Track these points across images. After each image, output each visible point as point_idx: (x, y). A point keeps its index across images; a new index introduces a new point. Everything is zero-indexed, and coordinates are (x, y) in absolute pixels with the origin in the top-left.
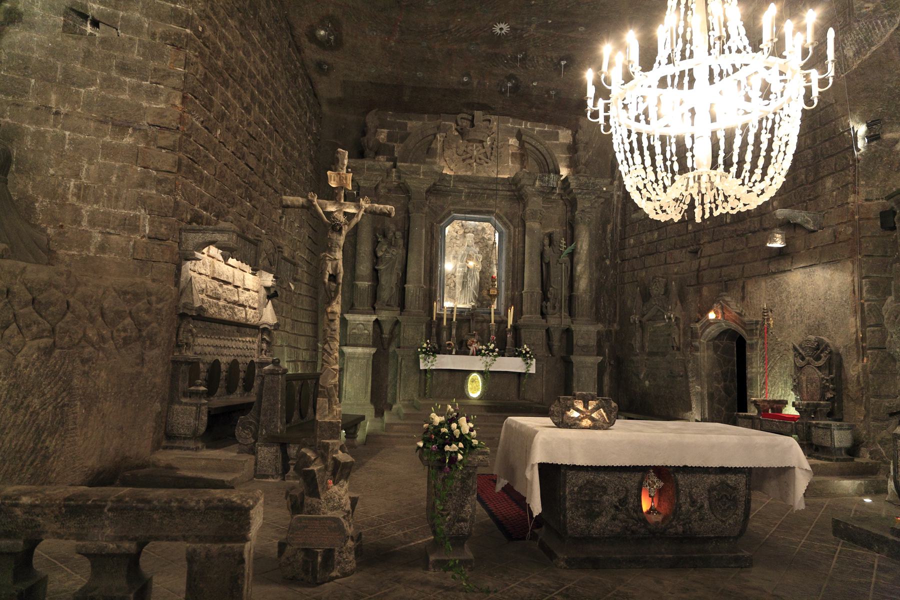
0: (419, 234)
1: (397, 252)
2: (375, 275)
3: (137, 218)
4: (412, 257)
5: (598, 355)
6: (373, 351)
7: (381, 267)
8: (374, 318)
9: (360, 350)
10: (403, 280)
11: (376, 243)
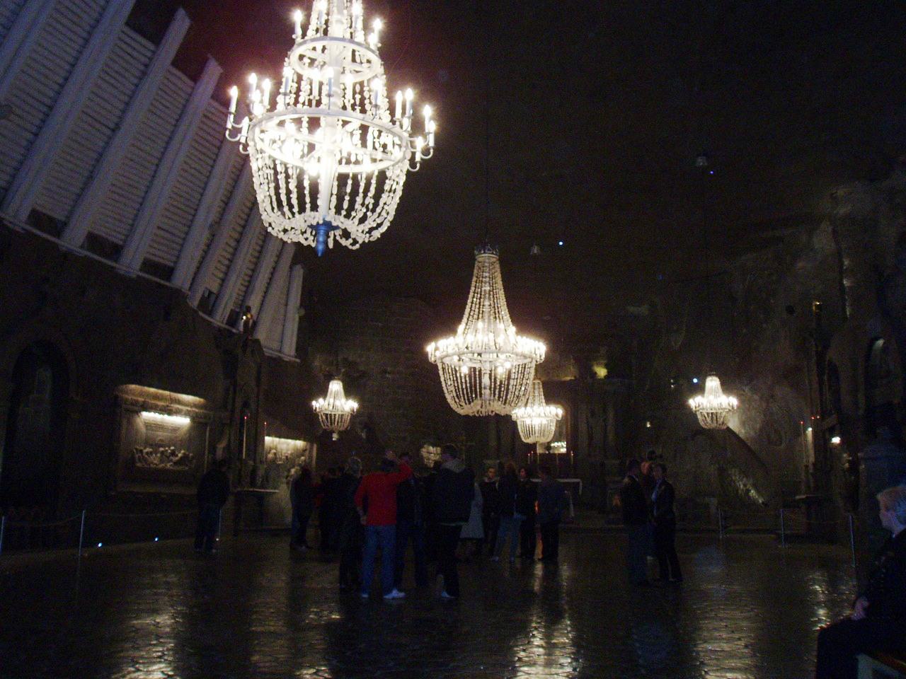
2: (499, 439)
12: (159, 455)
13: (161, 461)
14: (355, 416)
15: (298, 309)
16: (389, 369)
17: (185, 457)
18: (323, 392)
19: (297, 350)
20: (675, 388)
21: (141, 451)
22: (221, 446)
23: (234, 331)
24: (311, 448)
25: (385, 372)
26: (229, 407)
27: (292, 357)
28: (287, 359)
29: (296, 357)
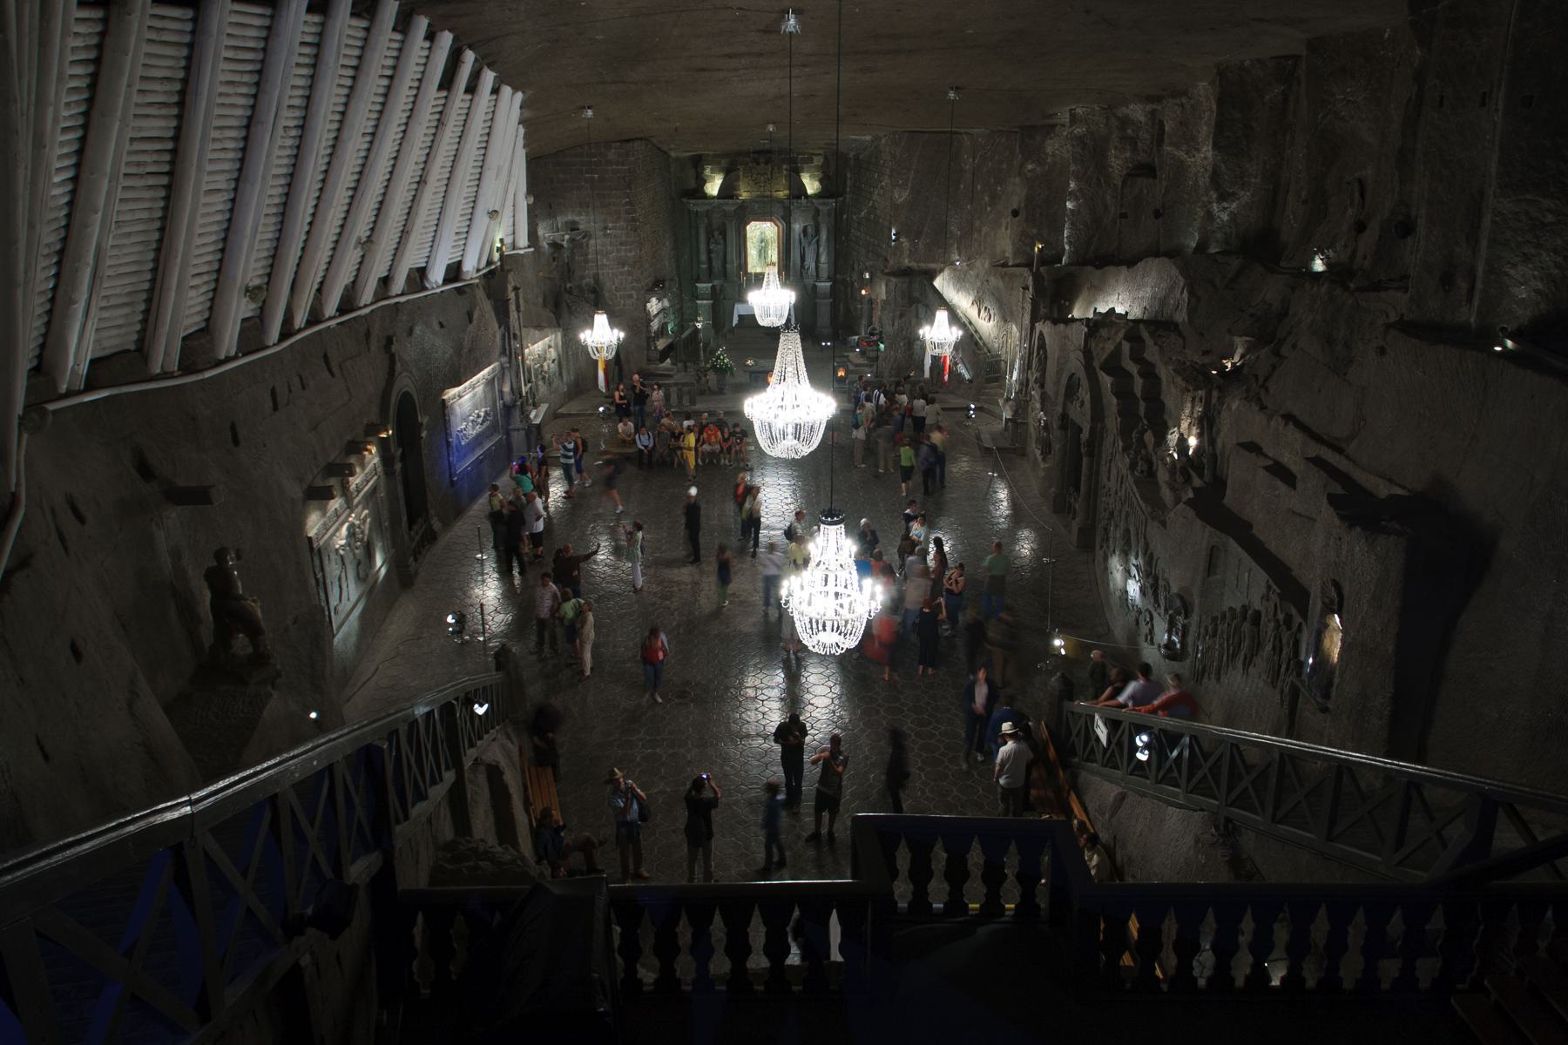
1: (721, 247)
2: (710, 260)
4: (729, 249)
5: (830, 298)
6: (711, 302)
7: (713, 255)
8: (711, 285)
9: (705, 302)
10: (725, 262)
12: (470, 424)
13: (473, 428)
15: (526, 198)
16: (610, 225)
17: (486, 412)
19: (529, 240)
20: (895, 245)
22: (507, 389)
23: (493, 267)
25: (606, 228)
26: (507, 352)
27: (525, 248)
28: (522, 252)
29: (529, 247)
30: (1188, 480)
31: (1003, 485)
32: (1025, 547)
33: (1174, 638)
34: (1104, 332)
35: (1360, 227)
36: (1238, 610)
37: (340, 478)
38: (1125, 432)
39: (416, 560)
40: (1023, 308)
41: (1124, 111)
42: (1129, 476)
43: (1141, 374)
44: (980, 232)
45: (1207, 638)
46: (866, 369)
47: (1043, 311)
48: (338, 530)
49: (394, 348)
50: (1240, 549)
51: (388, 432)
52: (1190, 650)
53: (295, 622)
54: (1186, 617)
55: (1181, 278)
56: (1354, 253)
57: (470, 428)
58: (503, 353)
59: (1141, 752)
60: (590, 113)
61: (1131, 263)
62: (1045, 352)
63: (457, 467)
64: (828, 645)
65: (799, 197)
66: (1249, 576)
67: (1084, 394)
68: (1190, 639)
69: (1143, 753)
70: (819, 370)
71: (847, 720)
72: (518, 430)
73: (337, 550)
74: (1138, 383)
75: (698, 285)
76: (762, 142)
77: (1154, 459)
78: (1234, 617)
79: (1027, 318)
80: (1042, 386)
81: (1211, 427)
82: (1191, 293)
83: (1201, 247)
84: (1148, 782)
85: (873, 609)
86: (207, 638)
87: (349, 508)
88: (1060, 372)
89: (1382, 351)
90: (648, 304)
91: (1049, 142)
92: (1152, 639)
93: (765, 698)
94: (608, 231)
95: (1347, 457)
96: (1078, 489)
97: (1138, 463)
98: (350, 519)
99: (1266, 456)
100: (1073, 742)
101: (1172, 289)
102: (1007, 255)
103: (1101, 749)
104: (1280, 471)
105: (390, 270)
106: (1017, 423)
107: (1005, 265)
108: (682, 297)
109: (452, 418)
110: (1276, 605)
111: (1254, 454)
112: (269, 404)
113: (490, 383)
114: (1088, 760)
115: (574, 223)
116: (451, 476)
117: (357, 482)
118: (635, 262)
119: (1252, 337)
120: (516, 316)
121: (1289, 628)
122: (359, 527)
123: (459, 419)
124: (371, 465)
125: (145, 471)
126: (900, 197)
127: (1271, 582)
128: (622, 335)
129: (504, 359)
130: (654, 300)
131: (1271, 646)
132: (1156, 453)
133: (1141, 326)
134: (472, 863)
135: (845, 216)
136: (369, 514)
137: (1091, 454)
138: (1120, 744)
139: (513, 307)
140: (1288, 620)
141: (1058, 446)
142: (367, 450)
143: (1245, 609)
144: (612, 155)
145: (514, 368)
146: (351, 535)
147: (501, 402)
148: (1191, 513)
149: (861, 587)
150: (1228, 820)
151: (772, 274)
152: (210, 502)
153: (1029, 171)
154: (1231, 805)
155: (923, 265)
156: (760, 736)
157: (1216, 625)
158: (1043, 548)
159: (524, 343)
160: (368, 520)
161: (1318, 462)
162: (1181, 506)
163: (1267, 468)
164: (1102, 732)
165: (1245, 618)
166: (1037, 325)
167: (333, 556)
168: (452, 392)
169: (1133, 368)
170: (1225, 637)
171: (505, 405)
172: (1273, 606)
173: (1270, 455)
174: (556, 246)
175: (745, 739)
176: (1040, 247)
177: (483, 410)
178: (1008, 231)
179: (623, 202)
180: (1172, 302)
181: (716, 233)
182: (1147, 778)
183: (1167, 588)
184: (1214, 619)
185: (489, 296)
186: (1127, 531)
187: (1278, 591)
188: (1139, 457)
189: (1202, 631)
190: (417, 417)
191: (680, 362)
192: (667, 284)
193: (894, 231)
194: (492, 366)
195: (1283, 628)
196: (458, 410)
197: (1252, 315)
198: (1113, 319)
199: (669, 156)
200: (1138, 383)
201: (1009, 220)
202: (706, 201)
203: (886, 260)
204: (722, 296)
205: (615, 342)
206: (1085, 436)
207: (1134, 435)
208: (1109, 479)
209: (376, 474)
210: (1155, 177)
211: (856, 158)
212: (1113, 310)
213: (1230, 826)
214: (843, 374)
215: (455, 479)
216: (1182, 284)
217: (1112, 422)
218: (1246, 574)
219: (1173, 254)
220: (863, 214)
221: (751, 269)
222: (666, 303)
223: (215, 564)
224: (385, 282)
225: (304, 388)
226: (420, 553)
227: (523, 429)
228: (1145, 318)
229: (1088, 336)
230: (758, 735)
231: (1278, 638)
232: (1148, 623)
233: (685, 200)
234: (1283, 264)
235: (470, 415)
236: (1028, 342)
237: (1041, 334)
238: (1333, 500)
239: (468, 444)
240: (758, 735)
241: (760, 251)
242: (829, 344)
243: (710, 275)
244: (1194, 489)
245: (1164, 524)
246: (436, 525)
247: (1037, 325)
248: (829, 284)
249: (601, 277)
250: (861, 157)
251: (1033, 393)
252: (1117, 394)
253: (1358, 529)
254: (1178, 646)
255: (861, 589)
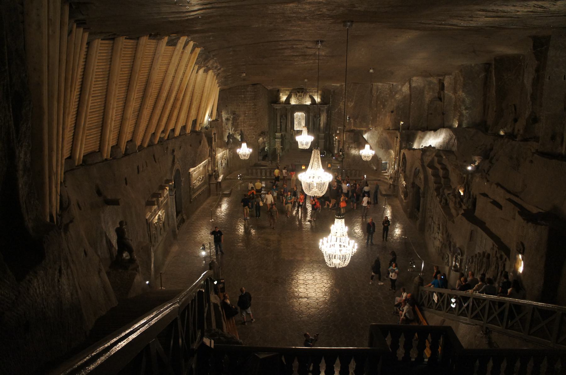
0: (289, 117)
2: (281, 125)
3: (253, 137)
4: (288, 121)
6: (281, 140)
7: (282, 124)
8: (281, 134)
9: (278, 140)
11: (280, 119)
13: (198, 183)
14: (251, 155)
16: (247, 113)
17: (202, 177)
18: (240, 146)
21: (194, 184)
22: (210, 169)
24: (227, 151)
26: (211, 156)
30: (461, 206)
31: (390, 208)
32: (398, 232)
33: (457, 264)
34: (428, 153)
35: (516, 120)
36: (482, 253)
37: (156, 198)
38: (437, 189)
39: (178, 229)
40: (396, 144)
41: (431, 79)
42: (439, 205)
43: (441, 168)
44: (379, 118)
45: (469, 264)
46: (338, 165)
47: (404, 145)
48: (155, 217)
49: (175, 153)
50: (482, 232)
51: (172, 182)
52: (463, 268)
53: (142, 249)
54: (462, 256)
55: (454, 135)
56: (514, 129)
57: (197, 183)
58: (210, 156)
59: (453, 304)
60: (244, 75)
61: (435, 130)
62: (405, 160)
63: (193, 196)
64: (336, 264)
65: (314, 104)
66: (485, 241)
67: (422, 176)
68: (463, 264)
69: (454, 305)
70: (326, 164)
71: (338, 293)
72: (213, 184)
73: (154, 224)
74: (441, 172)
75: (276, 134)
76: (301, 85)
77: (448, 199)
78: (480, 256)
79: (398, 148)
80: (405, 172)
81: (468, 188)
82: (458, 140)
83: (460, 125)
84: (454, 315)
85: (353, 251)
86: (115, 253)
87: (159, 209)
88: (412, 167)
89: (531, 162)
90: (259, 140)
91: (403, 88)
92: (448, 264)
93: (307, 283)
94: (246, 115)
95: (521, 199)
96: (418, 209)
97: (442, 200)
98: (159, 213)
99: (490, 198)
100: (423, 301)
101: (450, 139)
102: (389, 126)
103: (435, 304)
104: (495, 203)
105: (175, 126)
106: (395, 186)
107: (389, 129)
108: (270, 138)
109: (192, 179)
110: (496, 252)
111: (486, 197)
112: (136, 171)
113: (205, 167)
114: (429, 308)
115: (235, 111)
116: (190, 199)
117: (162, 199)
118: (255, 126)
119: (481, 156)
120: (214, 143)
121: (501, 260)
122: (161, 216)
123: (194, 180)
124: (166, 194)
125: (99, 193)
126: (350, 105)
127: (494, 243)
128: (251, 150)
129: (210, 158)
130: (261, 139)
131: (494, 267)
132: (449, 197)
133: (441, 152)
134: (217, 337)
135: (329, 112)
136: (165, 211)
137: (424, 197)
138: (443, 302)
139: (213, 140)
140: (501, 257)
141: (411, 194)
142: (166, 189)
143: (484, 253)
144: (249, 89)
145: (212, 162)
146: (159, 219)
147: (208, 173)
148: (464, 219)
149: (349, 244)
150: (487, 328)
151: (305, 131)
152: (118, 204)
153: (397, 98)
154: (488, 323)
155: (358, 129)
156: (306, 298)
157: (473, 259)
158: (404, 232)
159: (216, 153)
160: (164, 214)
161: (509, 200)
162: (460, 216)
163: (491, 202)
164: (435, 298)
165: (484, 256)
166: (402, 150)
167: (153, 226)
168: (192, 169)
169: (439, 166)
170: (476, 263)
171: (209, 174)
172: (495, 252)
173: (492, 198)
174: (227, 119)
175: (300, 299)
176: (402, 123)
177: (202, 176)
178: (390, 118)
179: (252, 105)
180: (451, 144)
181: (284, 116)
182: (454, 314)
183: (455, 246)
184: (472, 257)
185: (206, 137)
186: (439, 225)
187: (497, 246)
188: (443, 198)
189: (468, 261)
190: (180, 178)
191: (270, 161)
192: (266, 133)
193: (348, 117)
194: (205, 161)
195: (499, 259)
196: (193, 175)
197: (481, 149)
198: (431, 149)
199: (268, 90)
200: (441, 172)
201: (390, 114)
202: (281, 105)
203: (344, 126)
204: (285, 138)
205: (249, 153)
206: (422, 190)
207: (441, 190)
208: (431, 206)
209: (167, 198)
210: (441, 101)
211: (334, 92)
212: (430, 146)
213: (488, 330)
214: (330, 166)
215: (192, 200)
216: (454, 138)
217: (432, 185)
218: (485, 241)
219: (450, 127)
220: (336, 110)
221: (295, 129)
222: (265, 140)
223: (119, 226)
224: (173, 130)
225: (147, 166)
226: (179, 226)
227: (215, 183)
228: (441, 149)
229: (422, 155)
230: (305, 297)
231: (497, 264)
232: (446, 259)
233: (272, 105)
234: (489, 132)
235: (197, 178)
236: (398, 156)
237: (404, 154)
238: (518, 212)
239: (196, 188)
240: (305, 297)
241: (299, 123)
242: (323, 156)
243: (281, 130)
244: (464, 210)
245: (453, 222)
246: (185, 217)
247: (402, 150)
248: (323, 135)
249: (243, 130)
250: (336, 91)
251: (401, 175)
252: (433, 175)
253: (530, 224)
254: (459, 267)
255: (349, 244)
